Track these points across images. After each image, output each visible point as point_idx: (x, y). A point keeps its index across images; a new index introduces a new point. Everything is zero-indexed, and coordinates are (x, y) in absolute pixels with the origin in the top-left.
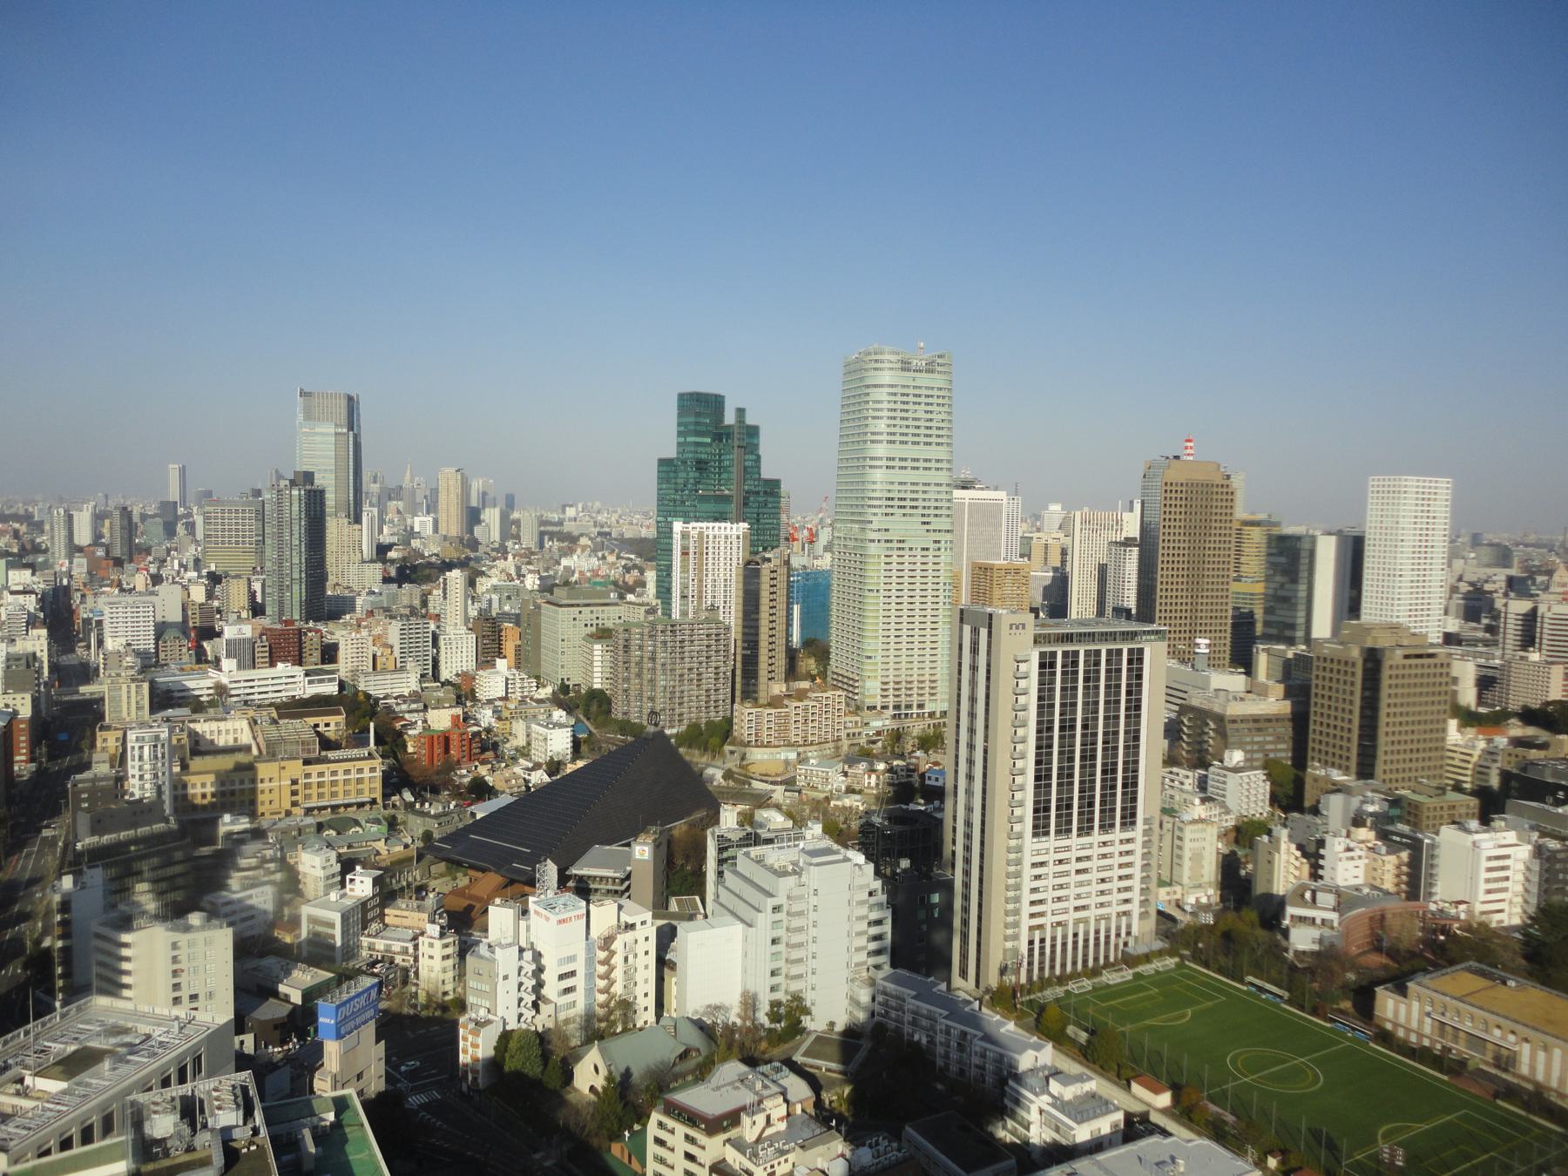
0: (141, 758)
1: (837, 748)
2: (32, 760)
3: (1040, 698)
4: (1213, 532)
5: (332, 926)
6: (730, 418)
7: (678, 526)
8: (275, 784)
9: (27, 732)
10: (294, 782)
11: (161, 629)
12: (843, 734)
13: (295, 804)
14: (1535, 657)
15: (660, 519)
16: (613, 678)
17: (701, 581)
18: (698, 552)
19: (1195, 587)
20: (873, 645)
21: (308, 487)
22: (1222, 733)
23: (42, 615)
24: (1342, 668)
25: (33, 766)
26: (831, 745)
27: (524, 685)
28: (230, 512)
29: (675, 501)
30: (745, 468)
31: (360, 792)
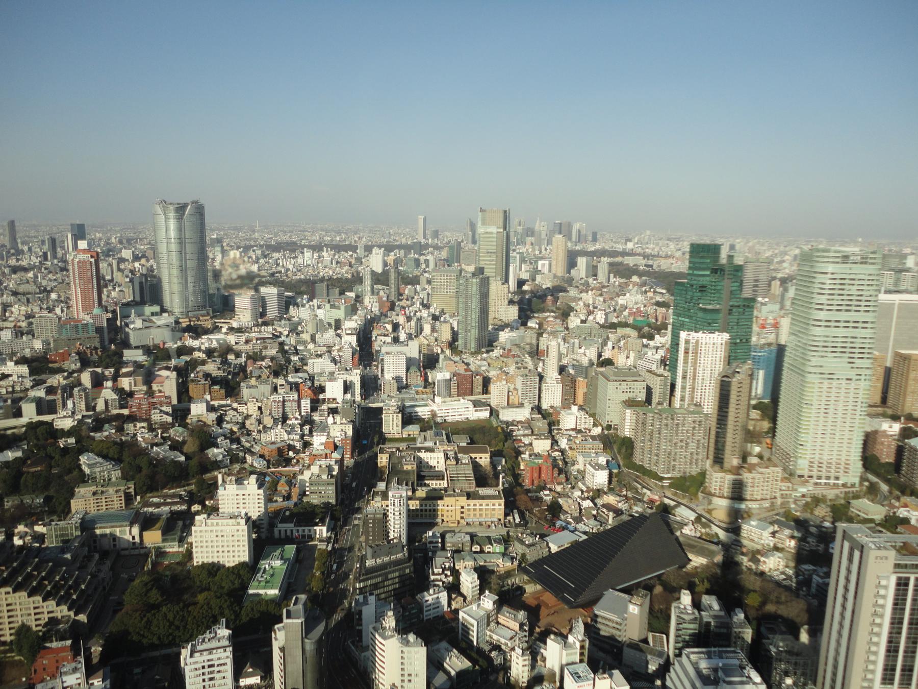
0: (394, 505)
1: (772, 503)
2: (352, 457)
3: (895, 604)
5: (473, 626)
6: (723, 258)
7: (683, 335)
8: (454, 508)
9: (350, 445)
10: (462, 507)
11: (410, 363)
12: (778, 495)
13: (462, 518)
15: (675, 317)
16: (635, 430)
17: (695, 369)
18: (694, 352)
20: (807, 437)
21: (481, 276)
23: (358, 349)
25: (353, 460)
26: (768, 501)
27: (586, 422)
28: (444, 276)
29: (684, 308)
30: (731, 292)
31: (493, 515)
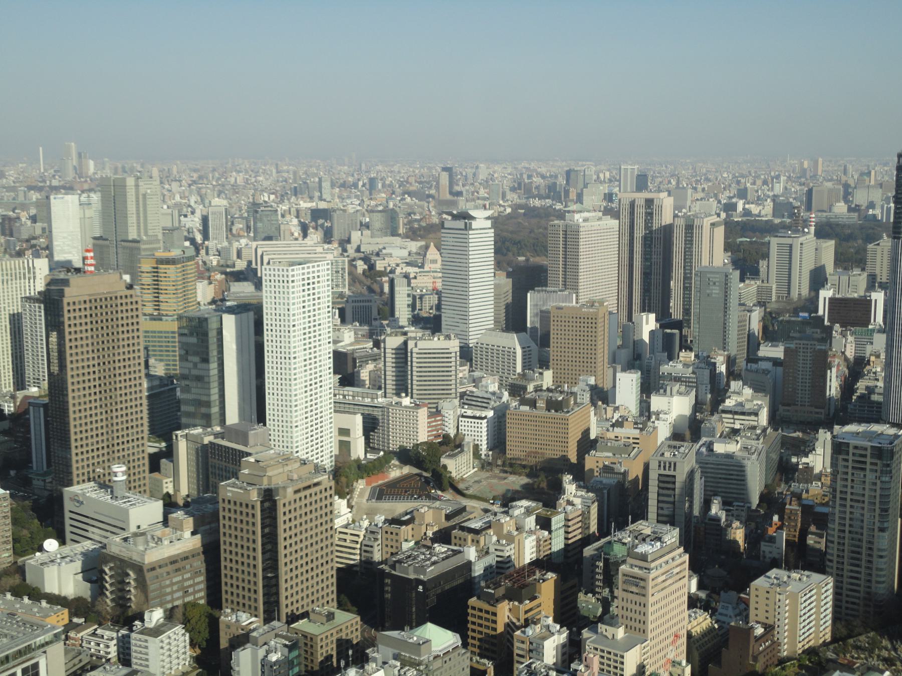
4: (121, 343)
14: (406, 401)
19: (109, 401)
22: (142, 584)
24: (244, 510)
